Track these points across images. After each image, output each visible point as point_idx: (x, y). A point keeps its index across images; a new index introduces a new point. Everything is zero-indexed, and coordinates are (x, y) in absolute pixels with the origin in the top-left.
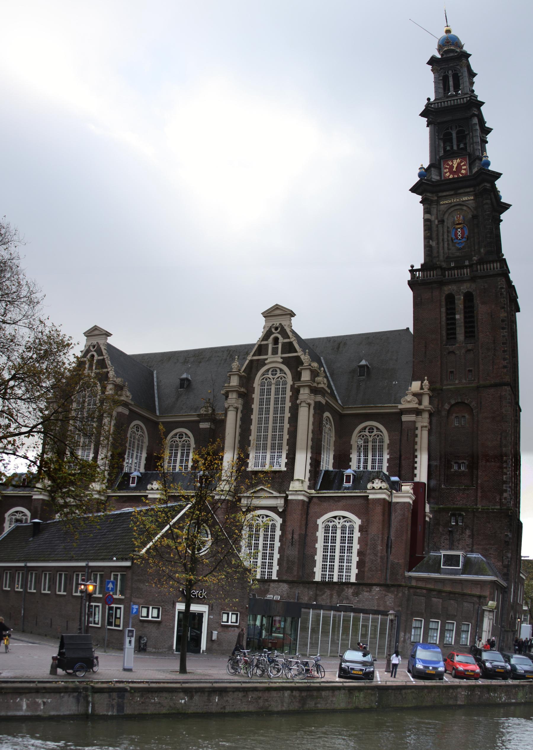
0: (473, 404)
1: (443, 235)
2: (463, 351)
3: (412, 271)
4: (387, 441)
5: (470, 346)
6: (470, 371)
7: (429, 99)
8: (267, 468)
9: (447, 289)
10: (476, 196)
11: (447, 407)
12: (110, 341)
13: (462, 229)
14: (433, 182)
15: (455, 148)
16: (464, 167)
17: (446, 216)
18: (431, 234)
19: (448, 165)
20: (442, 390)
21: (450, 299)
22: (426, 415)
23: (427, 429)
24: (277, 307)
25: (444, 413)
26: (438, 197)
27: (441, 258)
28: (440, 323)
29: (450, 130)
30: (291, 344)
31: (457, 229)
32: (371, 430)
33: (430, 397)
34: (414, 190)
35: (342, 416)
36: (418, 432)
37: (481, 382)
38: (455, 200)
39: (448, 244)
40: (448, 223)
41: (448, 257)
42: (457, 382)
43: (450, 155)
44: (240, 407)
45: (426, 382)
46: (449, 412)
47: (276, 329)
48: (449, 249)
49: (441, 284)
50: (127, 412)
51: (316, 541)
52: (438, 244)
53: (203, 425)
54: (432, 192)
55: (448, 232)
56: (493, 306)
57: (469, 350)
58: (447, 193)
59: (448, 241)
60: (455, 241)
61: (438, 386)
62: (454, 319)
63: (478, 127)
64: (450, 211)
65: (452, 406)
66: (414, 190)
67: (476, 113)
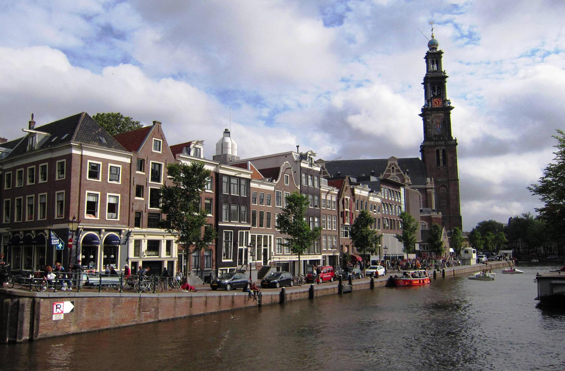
0: (447, 186)
5: (445, 167)
10: (445, 114)
11: (439, 186)
22: (434, 189)
24: (393, 157)
25: (438, 188)
26: (431, 113)
27: (433, 136)
36: (432, 194)
38: (438, 115)
40: (434, 123)
46: (439, 188)
47: (393, 164)
49: (435, 146)
65: (440, 186)
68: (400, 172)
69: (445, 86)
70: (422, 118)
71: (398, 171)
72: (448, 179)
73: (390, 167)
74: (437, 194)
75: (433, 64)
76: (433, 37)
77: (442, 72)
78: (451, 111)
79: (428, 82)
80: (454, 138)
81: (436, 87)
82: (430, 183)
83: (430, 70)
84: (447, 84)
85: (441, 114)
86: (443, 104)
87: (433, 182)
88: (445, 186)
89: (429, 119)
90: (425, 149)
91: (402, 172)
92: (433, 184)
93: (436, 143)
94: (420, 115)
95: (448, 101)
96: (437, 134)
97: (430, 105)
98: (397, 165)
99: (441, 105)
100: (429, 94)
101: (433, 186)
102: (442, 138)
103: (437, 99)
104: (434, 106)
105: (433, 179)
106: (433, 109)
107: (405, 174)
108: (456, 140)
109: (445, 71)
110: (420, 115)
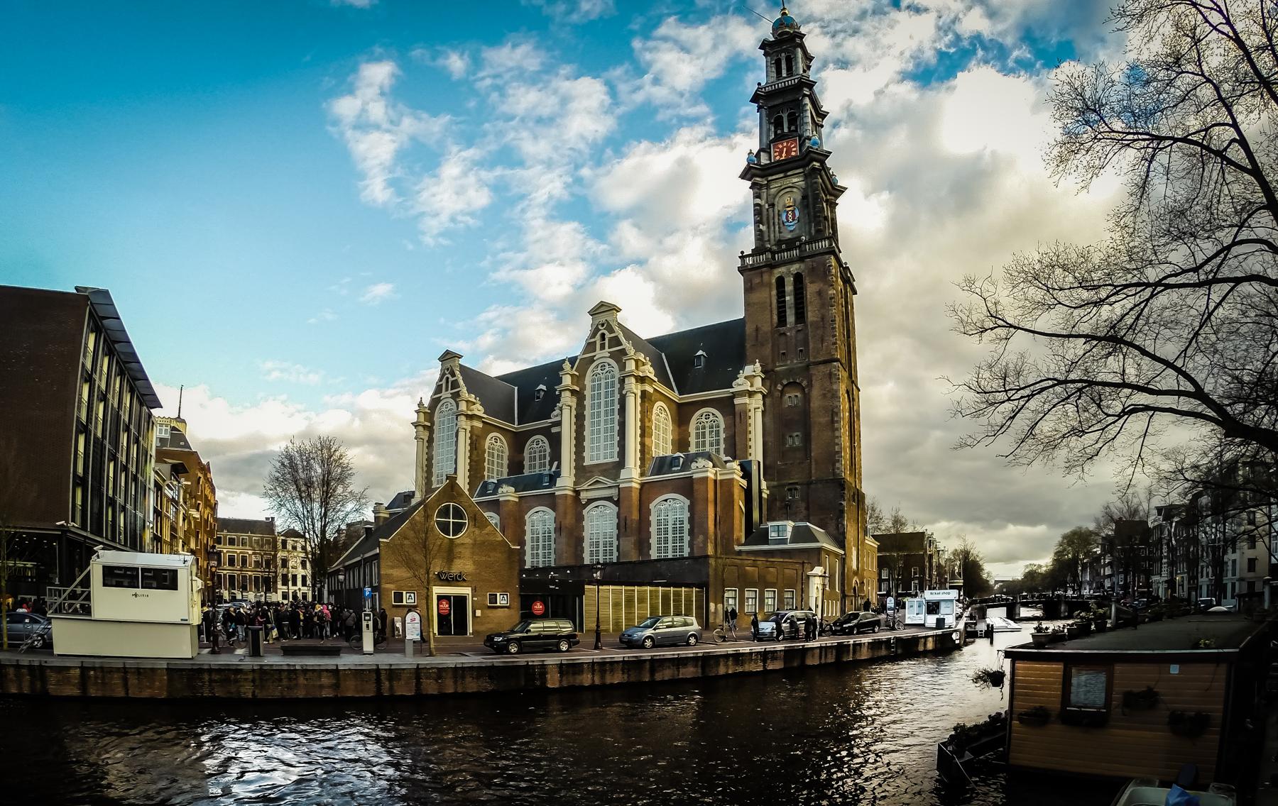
1: (774, 219)
2: (794, 332)
3: (743, 257)
5: (800, 326)
6: (801, 351)
7: (759, 84)
8: (602, 461)
10: (806, 177)
12: (461, 361)
13: (793, 211)
14: (760, 165)
15: (786, 130)
16: (794, 149)
17: (777, 199)
18: (761, 219)
19: (778, 148)
20: (773, 371)
21: (781, 282)
22: (760, 396)
23: (760, 410)
25: (777, 394)
26: (768, 181)
27: (773, 242)
28: (771, 306)
29: (781, 114)
31: (788, 212)
32: (707, 417)
33: (763, 379)
34: (743, 176)
35: (680, 406)
36: (751, 414)
37: (811, 360)
39: (779, 228)
40: (779, 207)
41: (779, 241)
42: (789, 362)
43: (779, 138)
44: (574, 406)
45: (758, 365)
48: (780, 232)
49: (772, 266)
50: (480, 425)
51: (649, 524)
52: (769, 227)
53: (554, 430)
55: (779, 215)
56: (822, 285)
57: (799, 331)
59: (779, 224)
60: (786, 224)
61: (770, 367)
62: (784, 301)
63: (809, 107)
64: (780, 194)
65: (784, 386)
66: (743, 176)
67: (808, 93)
88: (800, 384)
92: (758, 383)
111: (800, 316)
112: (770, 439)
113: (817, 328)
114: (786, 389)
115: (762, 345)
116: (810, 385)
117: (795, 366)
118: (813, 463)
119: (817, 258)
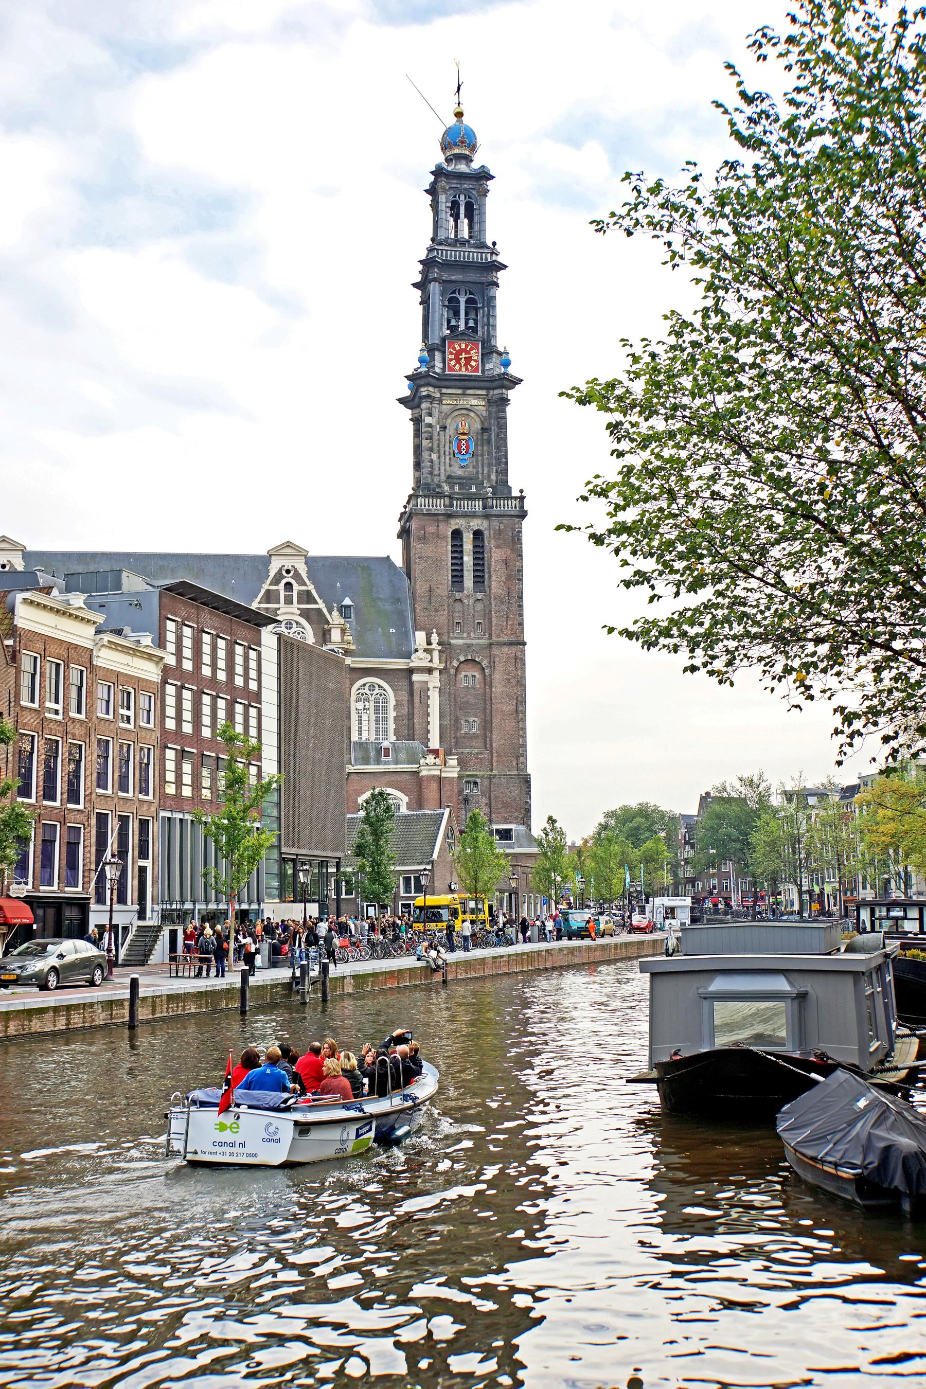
0: (485, 663)
2: (472, 600)
4: (392, 702)
5: (479, 596)
9: (455, 524)
10: (489, 402)
11: (455, 664)
17: (449, 420)
19: (454, 349)
21: (457, 535)
24: (288, 545)
25: (452, 671)
27: (443, 478)
30: (308, 592)
36: (429, 693)
37: (494, 639)
38: (463, 402)
40: (450, 431)
42: (465, 635)
46: (457, 669)
47: (288, 572)
49: (449, 516)
54: (435, 387)
58: (453, 391)
61: (445, 638)
68: (313, 601)
69: (494, 298)
70: (408, 413)
71: (306, 597)
72: (490, 638)
73: (276, 581)
74: (448, 692)
75: (456, 218)
76: (459, 115)
77: (484, 246)
78: (511, 394)
79: (435, 280)
80: (515, 493)
81: (462, 300)
82: (425, 650)
83: (442, 235)
84: (501, 295)
85: (474, 402)
86: (483, 366)
87: (435, 645)
89: (430, 415)
90: (414, 525)
91: (321, 605)
92: (436, 655)
93: (451, 506)
94: (401, 401)
95: (500, 354)
96: (460, 473)
97: (438, 365)
98: (304, 575)
99: (476, 370)
100: (437, 324)
101: (436, 663)
102: (473, 489)
103: (463, 346)
104: (451, 369)
105: (435, 638)
106: (443, 381)
107: (330, 611)
108: (522, 498)
109: (494, 244)
110: (401, 401)
111: (479, 579)
112: (447, 722)
113: (502, 602)
114: (462, 666)
115: (436, 610)
116: (492, 664)
117: (474, 642)
118: (495, 755)
119: (505, 520)
